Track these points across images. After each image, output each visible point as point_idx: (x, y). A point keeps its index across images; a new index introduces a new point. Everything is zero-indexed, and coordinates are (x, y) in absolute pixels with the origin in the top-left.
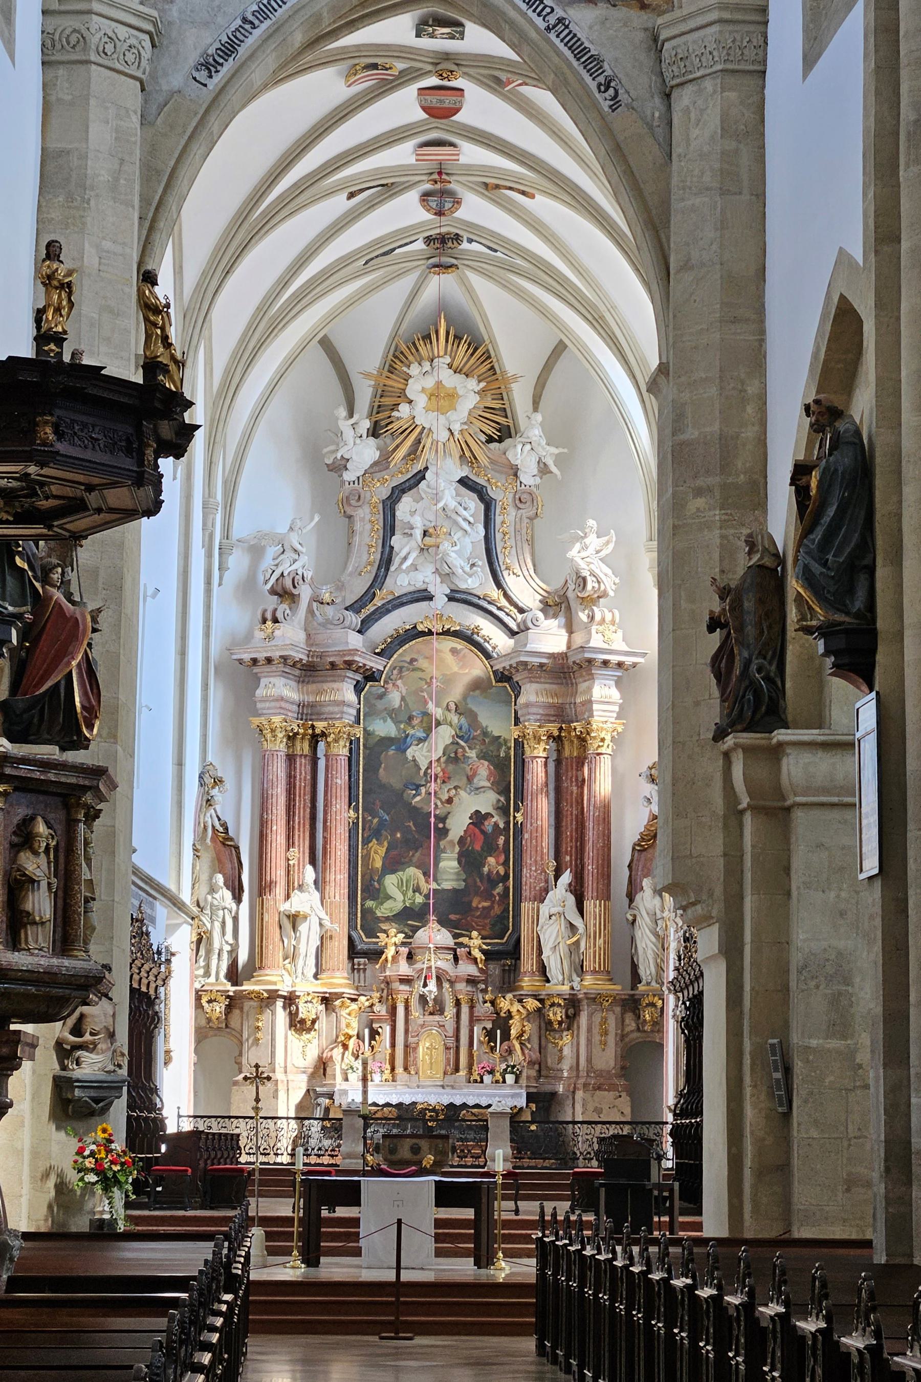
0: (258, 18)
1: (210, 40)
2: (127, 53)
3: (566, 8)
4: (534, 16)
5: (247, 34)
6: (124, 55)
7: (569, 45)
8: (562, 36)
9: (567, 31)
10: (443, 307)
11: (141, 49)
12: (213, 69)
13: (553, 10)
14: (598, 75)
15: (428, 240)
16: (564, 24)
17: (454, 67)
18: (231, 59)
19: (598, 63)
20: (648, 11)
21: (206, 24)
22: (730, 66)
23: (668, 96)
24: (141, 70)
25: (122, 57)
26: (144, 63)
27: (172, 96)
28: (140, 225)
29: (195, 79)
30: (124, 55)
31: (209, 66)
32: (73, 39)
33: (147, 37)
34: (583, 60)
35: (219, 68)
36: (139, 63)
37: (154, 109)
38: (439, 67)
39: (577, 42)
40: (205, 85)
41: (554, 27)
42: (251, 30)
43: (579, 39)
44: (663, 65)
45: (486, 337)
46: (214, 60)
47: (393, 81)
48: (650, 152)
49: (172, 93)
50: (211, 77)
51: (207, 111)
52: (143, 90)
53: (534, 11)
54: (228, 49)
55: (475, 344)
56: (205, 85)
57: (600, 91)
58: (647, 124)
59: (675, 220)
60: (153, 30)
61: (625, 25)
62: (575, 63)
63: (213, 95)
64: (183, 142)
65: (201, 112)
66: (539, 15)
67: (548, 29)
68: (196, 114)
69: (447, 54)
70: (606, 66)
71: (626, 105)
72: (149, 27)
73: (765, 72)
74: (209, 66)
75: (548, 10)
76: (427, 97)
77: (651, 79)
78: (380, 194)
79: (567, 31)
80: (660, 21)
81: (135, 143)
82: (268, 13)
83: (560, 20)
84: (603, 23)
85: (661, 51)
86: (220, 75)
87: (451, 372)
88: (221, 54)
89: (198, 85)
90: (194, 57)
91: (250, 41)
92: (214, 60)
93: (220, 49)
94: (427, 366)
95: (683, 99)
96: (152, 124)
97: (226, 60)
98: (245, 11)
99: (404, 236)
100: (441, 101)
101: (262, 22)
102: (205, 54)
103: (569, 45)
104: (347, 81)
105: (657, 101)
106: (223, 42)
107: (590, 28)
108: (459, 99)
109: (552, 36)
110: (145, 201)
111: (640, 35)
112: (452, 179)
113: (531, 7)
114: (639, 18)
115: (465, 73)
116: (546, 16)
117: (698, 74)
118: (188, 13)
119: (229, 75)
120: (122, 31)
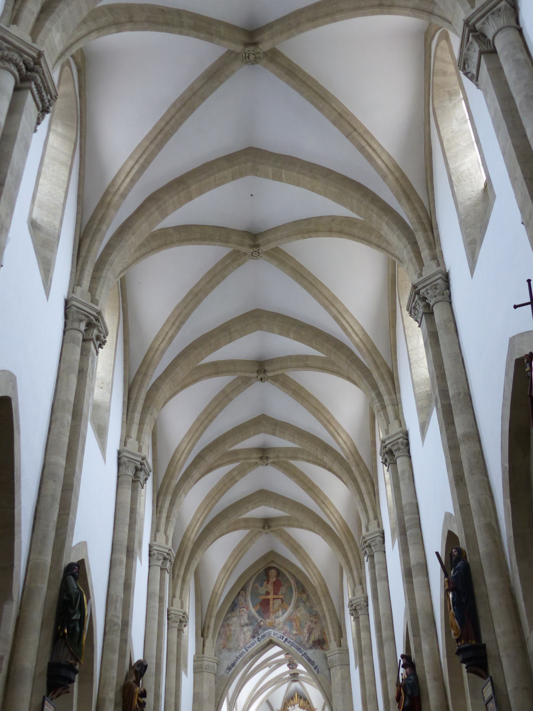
4: (299, 653)
10: (296, 691)
15: (291, 675)
22: (342, 663)
23: (330, 669)
26: (215, 669)
28: (215, 708)
31: (229, 669)
32: (200, 667)
40: (228, 673)
44: (328, 662)
45: (308, 698)
50: (230, 671)
52: (215, 675)
54: (233, 665)
55: (305, 700)
59: (333, 700)
62: (309, 663)
67: (302, 655)
70: (315, 663)
72: (216, 661)
73: (349, 664)
74: (229, 669)
75: (302, 651)
80: (326, 652)
83: (305, 653)
86: (232, 671)
87: (299, 708)
90: (226, 667)
91: (238, 662)
94: (293, 707)
95: (333, 670)
99: (284, 674)
102: (228, 666)
105: (327, 671)
109: (303, 657)
110: (216, 702)
114: (321, 651)
117: (335, 665)
120: (210, 663)
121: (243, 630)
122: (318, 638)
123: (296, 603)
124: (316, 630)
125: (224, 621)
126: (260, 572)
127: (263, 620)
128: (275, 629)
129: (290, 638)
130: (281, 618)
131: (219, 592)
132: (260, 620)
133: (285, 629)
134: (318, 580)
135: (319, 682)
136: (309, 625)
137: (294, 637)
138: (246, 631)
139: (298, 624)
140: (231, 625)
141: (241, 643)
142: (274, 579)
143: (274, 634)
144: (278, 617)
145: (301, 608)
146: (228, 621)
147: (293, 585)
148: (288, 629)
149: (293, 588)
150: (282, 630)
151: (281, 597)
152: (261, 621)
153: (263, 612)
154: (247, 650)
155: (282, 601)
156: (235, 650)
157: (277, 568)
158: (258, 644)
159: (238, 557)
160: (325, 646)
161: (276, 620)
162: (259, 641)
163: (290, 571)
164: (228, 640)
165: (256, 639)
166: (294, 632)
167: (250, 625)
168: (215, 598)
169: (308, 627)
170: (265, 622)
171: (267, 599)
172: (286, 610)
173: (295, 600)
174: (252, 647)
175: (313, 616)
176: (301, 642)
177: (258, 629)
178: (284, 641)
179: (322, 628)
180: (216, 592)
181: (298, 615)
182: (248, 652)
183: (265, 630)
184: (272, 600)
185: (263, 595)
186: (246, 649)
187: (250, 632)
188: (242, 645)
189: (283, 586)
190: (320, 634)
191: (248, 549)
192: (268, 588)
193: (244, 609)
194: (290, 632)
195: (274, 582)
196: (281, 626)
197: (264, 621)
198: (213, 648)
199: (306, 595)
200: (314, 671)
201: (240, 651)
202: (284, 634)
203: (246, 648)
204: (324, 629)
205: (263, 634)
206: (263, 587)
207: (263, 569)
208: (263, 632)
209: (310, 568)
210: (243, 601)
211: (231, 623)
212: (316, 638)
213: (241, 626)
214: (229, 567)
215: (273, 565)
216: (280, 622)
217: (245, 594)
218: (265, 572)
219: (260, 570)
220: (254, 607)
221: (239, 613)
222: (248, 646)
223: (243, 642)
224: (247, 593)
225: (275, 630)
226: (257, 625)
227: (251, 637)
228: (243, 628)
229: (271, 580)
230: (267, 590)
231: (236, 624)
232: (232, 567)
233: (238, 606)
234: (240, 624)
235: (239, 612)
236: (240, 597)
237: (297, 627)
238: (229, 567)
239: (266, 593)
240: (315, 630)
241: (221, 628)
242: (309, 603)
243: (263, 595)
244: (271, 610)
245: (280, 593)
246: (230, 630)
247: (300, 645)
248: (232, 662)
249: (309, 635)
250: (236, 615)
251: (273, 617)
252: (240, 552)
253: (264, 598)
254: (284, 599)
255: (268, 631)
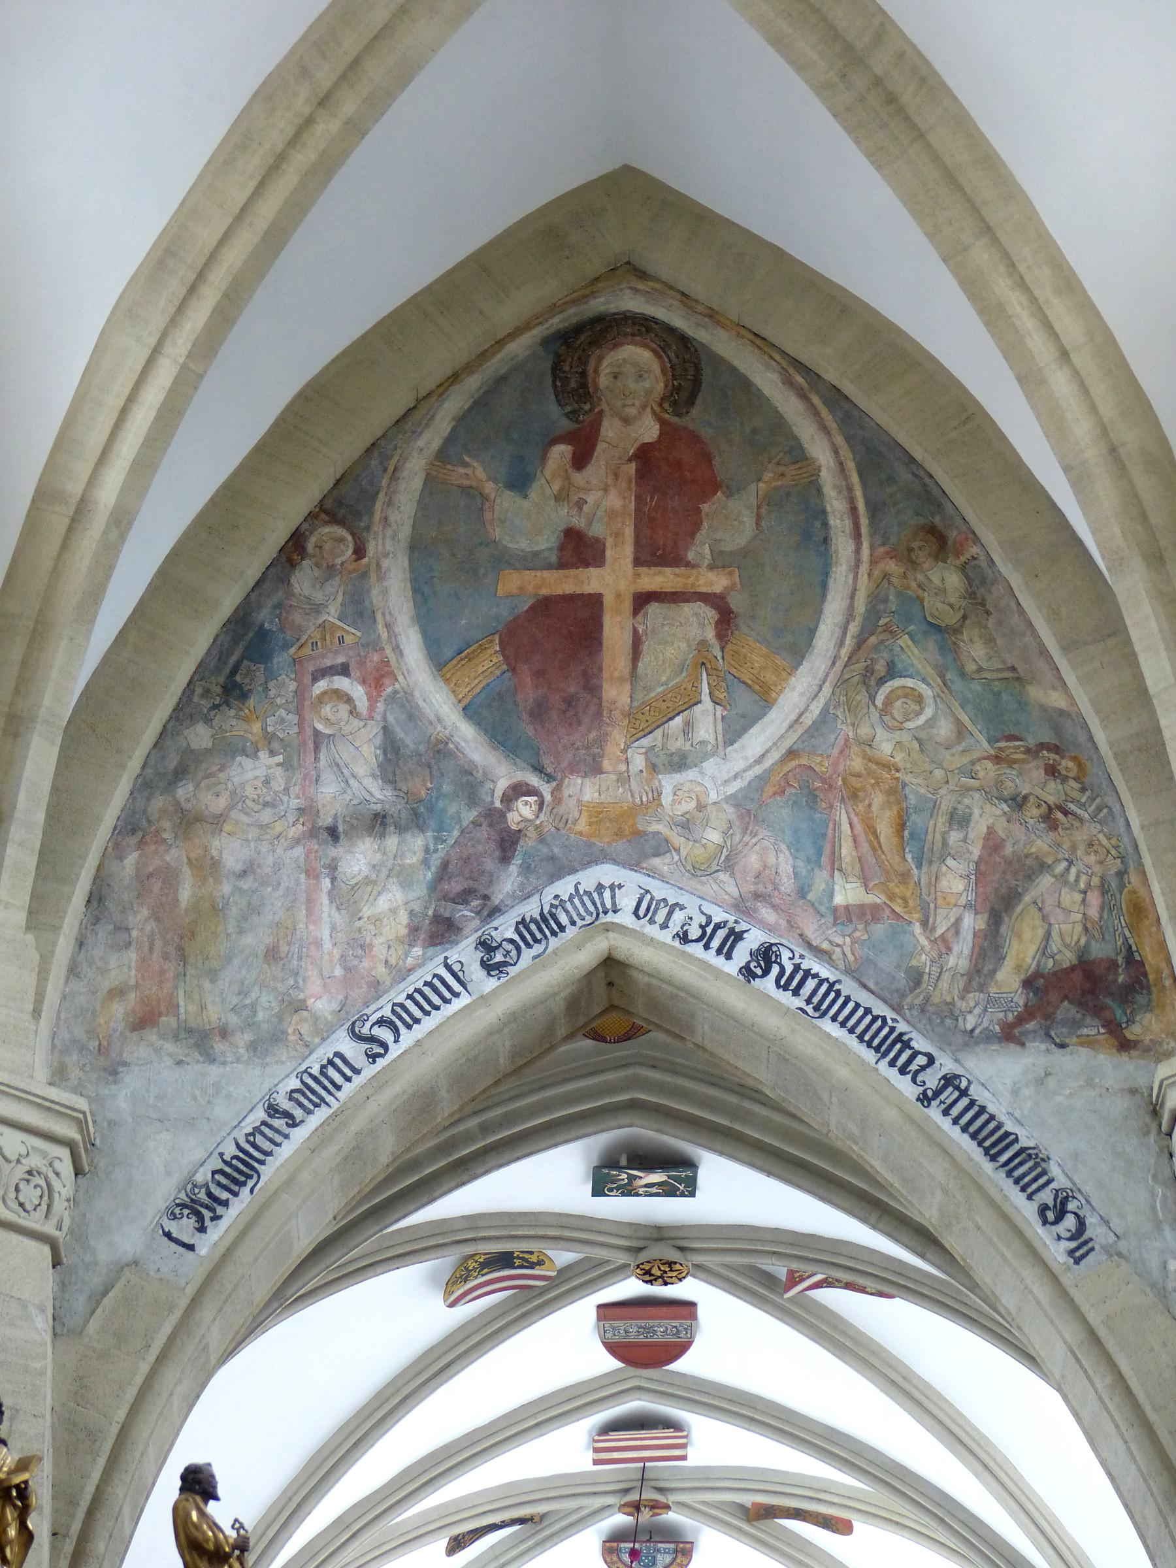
0: (301, 1105)
1: (200, 1154)
2: (22, 1186)
3: (960, 1055)
4: (892, 1074)
5: (278, 1139)
6: (17, 1189)
7: (972, 1129)
8: (955, 1112)
9: (964, 1102)
11: (51, 1175)
12: (207, 1214)
13: (931, 1060)
14: (1038, 1190)
16: (957, 1088)
17: (674, 1255)
18: (245, 1191)
19: (1037, 1165)
20: (1134, 1053)
21: (191, 1123)
24: (53, 1221)
25: (12, 1195)
26: (59, 1206)
27: (122, 1269)
29: (168, 1235)
30: (17, 1189)
33: (65, 1153)
34: (1004, 1158)
35: (220, 1210)
36: (49, 1206)
37: (80, 1303)
38: (643, 1257)
39: (988, 1122)
40: (191, 1248)
41: (937, 1093)
42: (286, 1130)
43: (992, 1118)
46: (210, 1194)
47: (544, 1291)
48: (1164, 1344)
49: (120, 1268)
50: (202, 1229)
51: (196, 1301)
52: (56, 1263)
53: (892, 1064)
56: (191, 1248)
57: (1045, 1222)
58: (1153, 1285)
60: (77, 1137)
61: (1090, 1084)
62: (988, 1166)
63: (208, 1267)
64: (144, 1368)
65: (184, 1302)
66: (903, 1071)
67: (925, 1099)
68: (171, 1309)
69: (659, 1228)
70: (1054, 1170)
71: (1107, 1250)
72: (71, 1132)
75: (921, 1060)
76: (616, 1323)
77: (1153, 1195)
78: (515, 1541)
79: (964, 1102)
81: (42, 1373)
82: (323, 1093)
83: (949, 1080)
84: (1040, 1082)
85: (1170, 1135)
86: (224, 1224)
88: (224, 1181)
89: (175, 1247)
90: (165, 1191)
91: (286, 1151)
92: (210, 1194)
93: (221, 1172)
96: (79, 1332)
97: (236, 1194)
98: (272, 1092)
100: (649, 1330)
101: (309, 1112)
103: (972, 1129)
104: (448, 1293)
106: (227, 1157)
107: (1015, 1092)
108: (688, 1322)
109: (934, 1112)
111: (1122, 1104)
112: (671, 1499)
113: (884, 1055)
115: (698, 1266)
116: (917, 1073)
118: (152, 1100)
119: (240, 1226)
121: (333, 868)
122: (1082, 953)
123: (860, 644)
124: (1062, 878)
125: (145, 785)
126: (495, 365)
127: (534, 780)
128: (656, 861)
129: (809, 945)
130: (710, 765)
131: (108, 493)
132: (502, 785)
133: (753, 861)
134: (1093, 408)
135: (1093, 1337)
136: (991, 831)
137: (839, 939)
138: (368, 881)
139: (885, 829)
140: (218, 821)
141: (314, 986)
142: (648, 430)
143: (645, 909)
144: (679, 763)
145: (909, 682)
146: (183, 791)
147: (828, 479)
148: (785, 865)
149: (835, 505)
150: (722, 876)
151: (716, 582)
152: (519, 790)
153: (539, 713)
154: (376, 1049)
155: (726, 620)
156: (253, 1046)
157: (671, 330)
158: (484, 999)
159: (302, 158)
160: (1148, 1018)
161: (668, 782)
162: (489, 967)
163: (804, 358)
164: (183, 958)
165: (465, 953)
166: (847, 893)
167: (401, 829)
168: (65, 546)
169: (976, 852)
170: (557, 800)
171: (572, 598)
172: (765, 698)
173: (850, 615)
174: (429, 1023)
175: (1033, 752)
176: (916, 978)
177: (489, 864)
178: (747, 972)
179: (1114, 866)
180: (76, 489)
181: (885, 747)
182: (381, 1063)
183: (557, 875)
184: (627, 605)
185: (530, 561)
186: (372, 1039)
187: (406, 885)
188: (323, 1006)
189: (729, 495)
190: (1093, 912)
191: (405, 76)
192: (581, 503)
193: (342, 683)
194: (802, 893)
195: (644, 454)
196: (714, 836)
197: (546, 789)
198: (37, 1013)
199: (963, 568)
200: (1042, 1235)
201: (310, 1048)
202: (741, 906)
203: (365, 1031)
204: (1134, 879)
205: (530, 909)
206: (534, 494)
207: (538, 333)
208: (539, 890)
209: (1022, 285)
210: (332, 614)
211: (218, 804)
212: (1055, 945)
213: (313, 833)
214: (212, 258)
215: (632, 303)
216: (701, 807)
217: (360, 552)
218: (556, 369)
219: (500, 343)
220: (440, 665)
221: (293, 718)
222: (387, 1012)
223: (338, 972)
224: (372, 548)
225: (652, 873)
226: (475, 824)
227: (414, 930)
228: (334, 852)
229: (610, 430)
230: (579, 522)
231: (266, 816)
232: (234, 257)
233: (281, 659)
234: (307, 811)
235: (299, 712)
236: (303, 581)
237: (876, 846)
238: (212, 258)
239: (562, 548)
240: (1046, 880)
241: (115, 848)
242: (990, 641)
243: (530, 561)
244: (616, 694)
245: (700, 550)
246: (208, 868)
247: (897, 1009)
248: (230, 1150)
249: (995, 919)
250: (269, 738)
251: (638, 762)
252: (324, 101)
253: (545, 591)
254: (736, 602)
255: (588, 878)
